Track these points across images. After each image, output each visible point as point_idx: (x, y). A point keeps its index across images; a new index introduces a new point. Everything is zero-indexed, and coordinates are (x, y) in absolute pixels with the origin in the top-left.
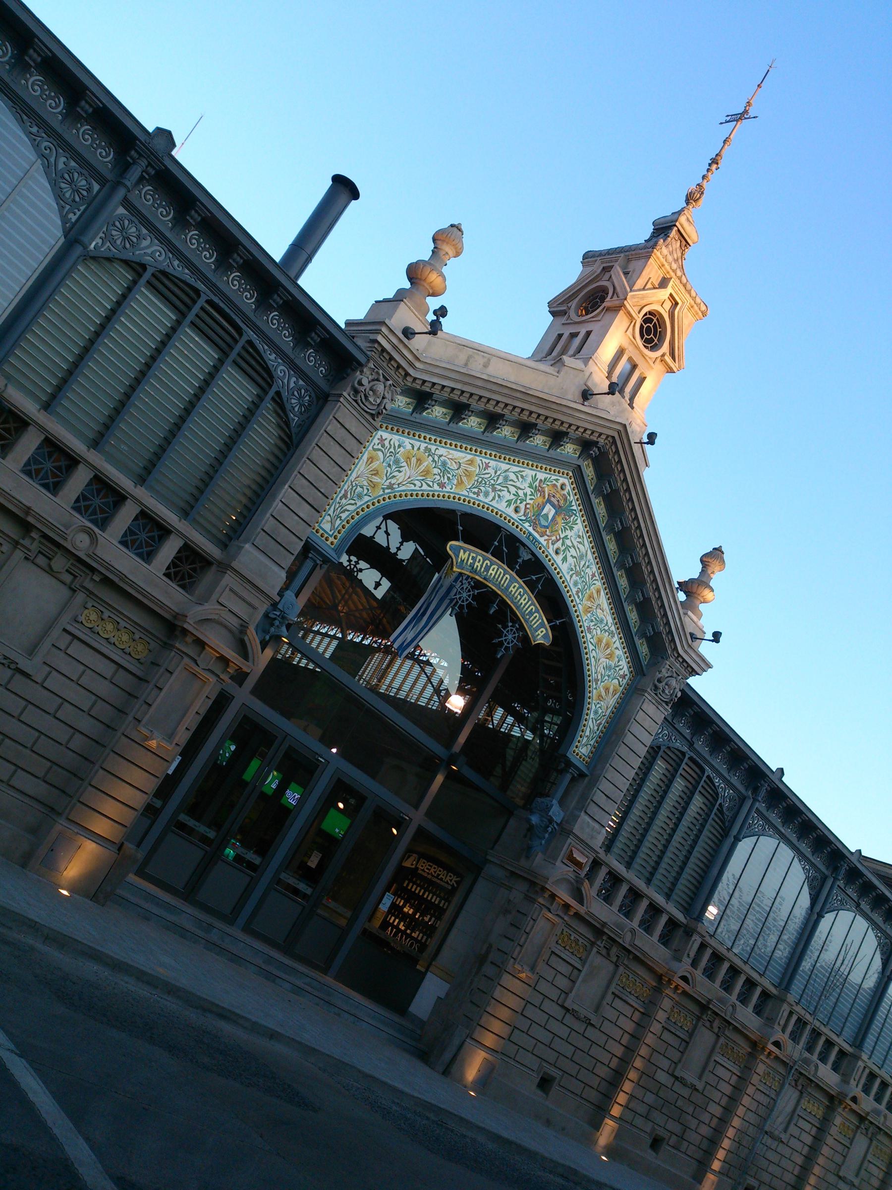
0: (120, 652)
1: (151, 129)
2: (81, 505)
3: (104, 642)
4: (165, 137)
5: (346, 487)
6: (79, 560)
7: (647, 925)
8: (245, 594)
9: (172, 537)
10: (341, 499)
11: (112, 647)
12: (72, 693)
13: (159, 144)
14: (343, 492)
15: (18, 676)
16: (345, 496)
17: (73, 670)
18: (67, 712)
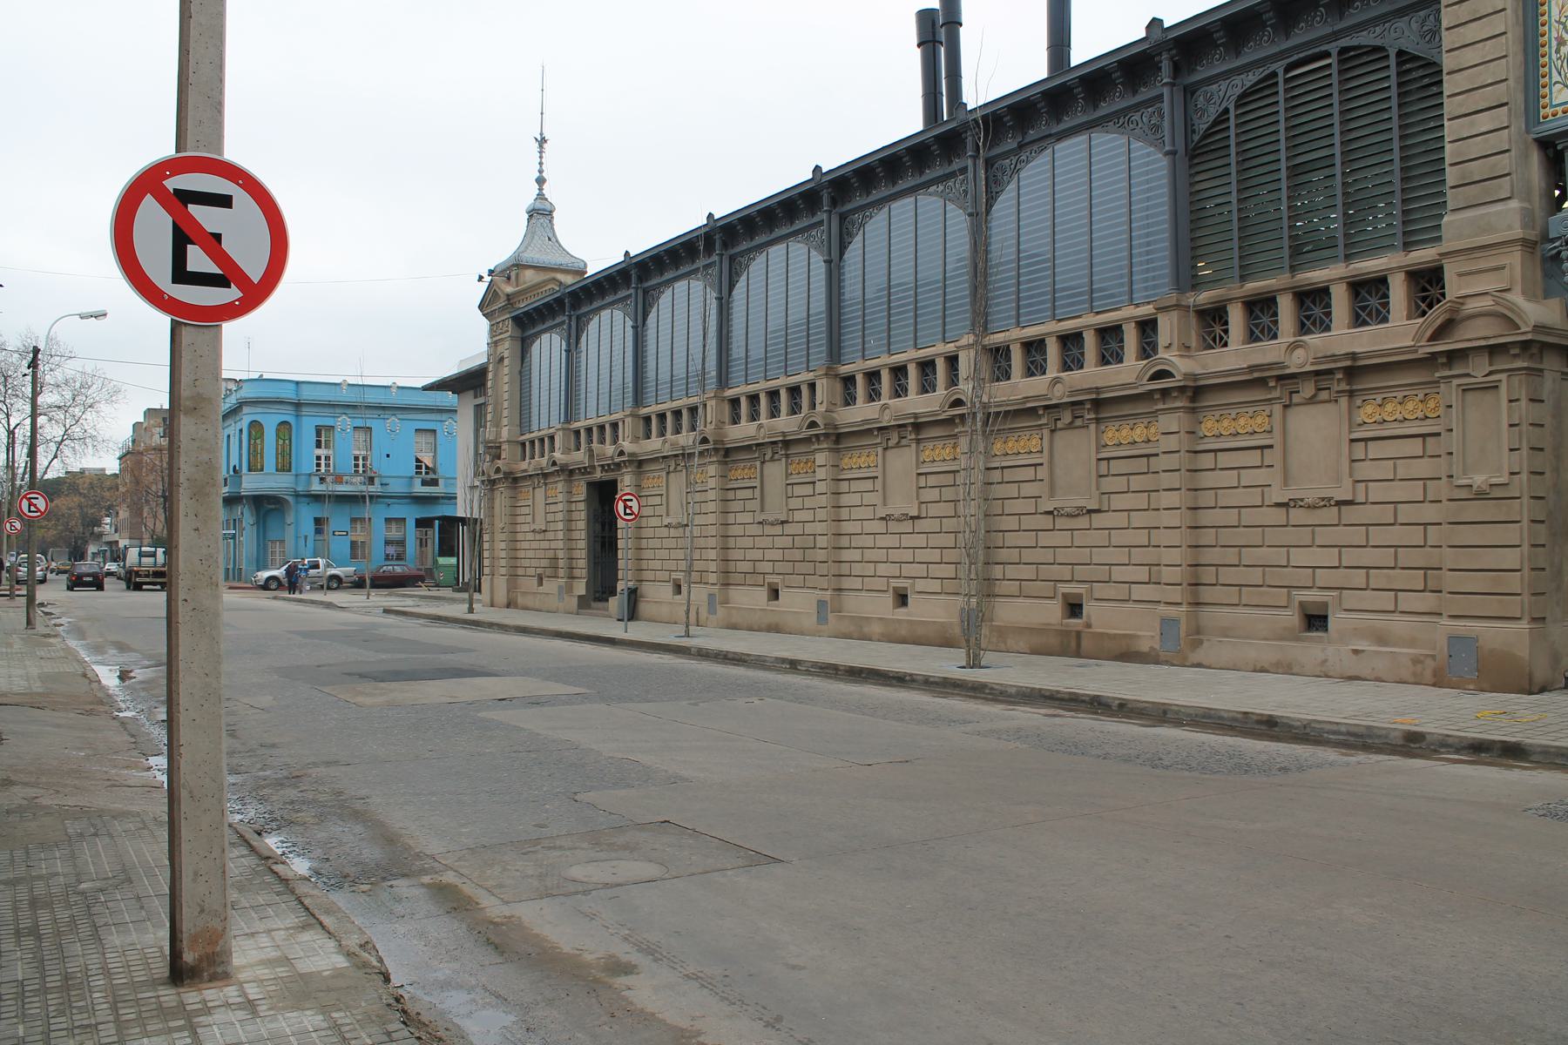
0: (1418, 423)
1: (1143, 35)
2: (1358, 320)
3: (1396, 425)
4: (1155, 23)
5: (1554, 34)
6: (1317, 373)
7: (1034, 367)
8: (1483, 265)
9: (1229, 308)
10: (1557, 51)
11: (1407, 424)
12: (1399, 492)
13: (1157, 35)
14: (1554, 43)
15: (1343, 508)
16: (1561, 42)
17: (1385, 470)
18: (1406, 514)
